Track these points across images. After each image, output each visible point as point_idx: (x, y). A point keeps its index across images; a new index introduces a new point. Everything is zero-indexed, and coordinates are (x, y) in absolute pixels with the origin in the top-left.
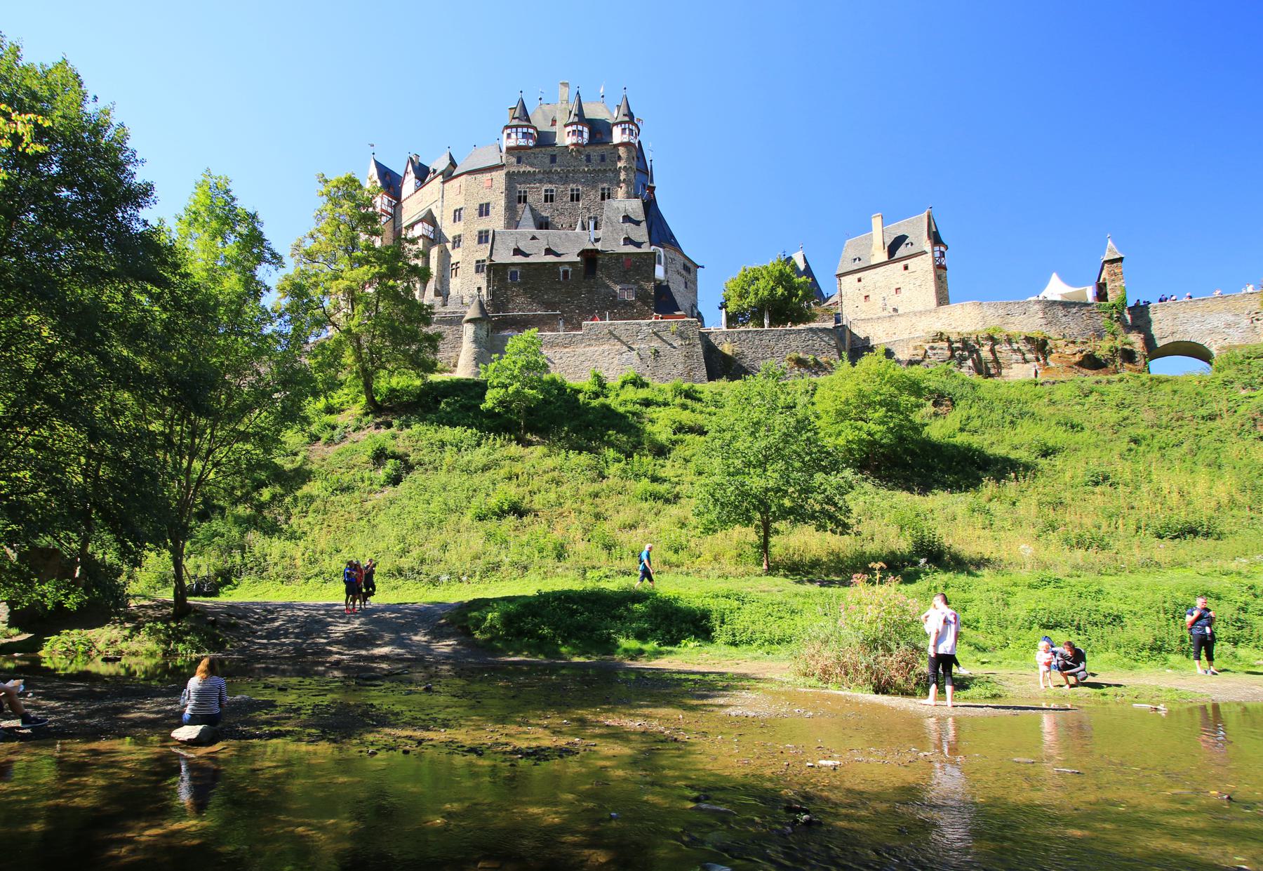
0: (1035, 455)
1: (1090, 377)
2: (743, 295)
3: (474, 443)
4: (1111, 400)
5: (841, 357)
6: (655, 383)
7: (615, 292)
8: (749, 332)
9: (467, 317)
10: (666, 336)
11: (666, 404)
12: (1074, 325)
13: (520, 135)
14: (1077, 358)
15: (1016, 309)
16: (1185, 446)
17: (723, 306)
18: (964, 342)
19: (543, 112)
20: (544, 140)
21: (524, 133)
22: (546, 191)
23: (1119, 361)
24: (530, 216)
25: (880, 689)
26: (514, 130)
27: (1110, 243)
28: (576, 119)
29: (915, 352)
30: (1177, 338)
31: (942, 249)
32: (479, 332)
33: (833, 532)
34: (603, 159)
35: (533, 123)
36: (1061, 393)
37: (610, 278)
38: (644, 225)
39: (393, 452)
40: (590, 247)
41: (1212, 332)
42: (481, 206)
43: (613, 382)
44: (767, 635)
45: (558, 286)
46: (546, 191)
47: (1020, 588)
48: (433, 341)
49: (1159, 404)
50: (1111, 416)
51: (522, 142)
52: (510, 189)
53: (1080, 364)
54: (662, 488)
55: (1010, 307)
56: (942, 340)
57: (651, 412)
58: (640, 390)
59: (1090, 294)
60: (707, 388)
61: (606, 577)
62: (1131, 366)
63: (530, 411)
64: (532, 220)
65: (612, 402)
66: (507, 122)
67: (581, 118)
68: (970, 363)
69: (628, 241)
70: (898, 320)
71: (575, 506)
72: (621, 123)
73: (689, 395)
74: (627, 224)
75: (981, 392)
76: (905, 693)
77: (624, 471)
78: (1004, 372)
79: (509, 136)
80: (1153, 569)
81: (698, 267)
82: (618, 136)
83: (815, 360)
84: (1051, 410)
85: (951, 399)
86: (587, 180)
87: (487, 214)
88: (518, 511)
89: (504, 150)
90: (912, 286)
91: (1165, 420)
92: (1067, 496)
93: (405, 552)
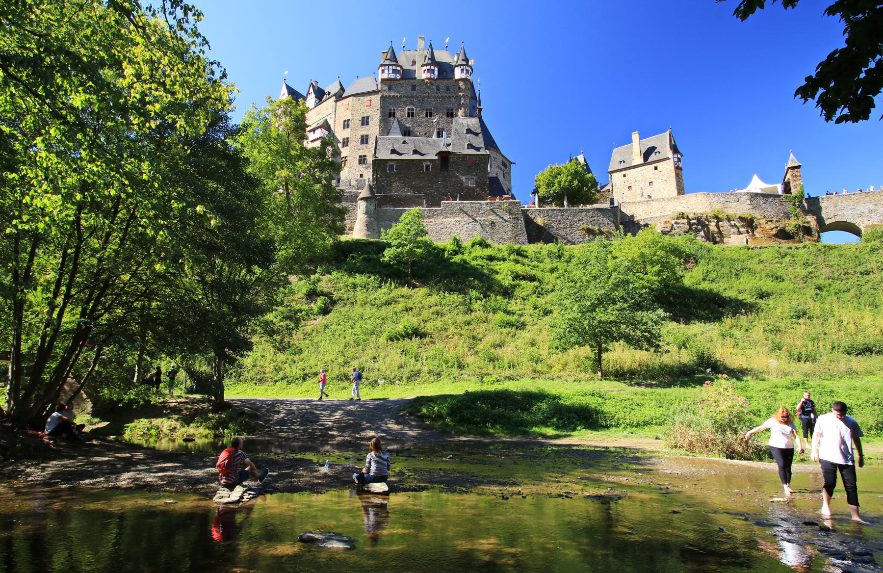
0: (755, 297)
1: (785, 245)
2: (550, 184)
3: (377, 285)
4: (800, 260)
6: (495, 245)
7: (462, 181)
8: (554, 210)
9: (361, 196)
10: (499, 212)
11: (504, 260)
12: (771, 210)
13: (391, 71)
14: (774, 232)
15: (732, 198)
16: (852, 292)
17: (536, 191)
19: (406, 56)
20: (408, 75)
21: (393, 70)
22: (409, 109)
23: (801, 234)
24: (398, 126)
26: (387, 67)
27: (791, 155)
28: (430, 62)
29: (665, 226)
30: (838, 219)
31: (679, 156)
32: (369, 206)
33: (647, 350)
34: (448, 89)
35: (400, 63)
36: (766, 255)
37: (458, 171)
38: (481, 135)
39: (322, 291)
40: (444, 149)
41: (860, 215)
42: (363, 118)
43: (466, 244)
45: (422, 176)
46: (409, 109)
47: (780, 389)
48: (342, 213)
49: (831, 264)
50: (801, 271)
51: (392, 76)
52: (383, 108)
53: (776, 236)
54: (513, 318)
55: (728, 196)
56: (683, 218)
57: (496, 265)
58: (485, 250)
59: (779, 189)
60: (531, 249)
61: (498, 381)
62: (809, 237)
63: (414, 263)
65: (466, 257)
66: (382, 63)
67: (433, 61)
68: (702, 233)
69: (470, 146)
71: (456, 331)
72: (460, 65)
73: (519, 253)
74: (469, 135)
75: (714, 254)
77: (484, 306)
78: (725, 240)
79: (383, 71)
80: (854, 376)
81: (512, 163)
82: (458, 74)
83: (599, 230)
84: (761, 266)
85: (695, 259)
86: (437, 103)
87: (367, 124)
88: (416, 333)
89: (379, 80)
90: (660, 181)
91: (836, 274)
92: (782, 325)
93: (346, 363)
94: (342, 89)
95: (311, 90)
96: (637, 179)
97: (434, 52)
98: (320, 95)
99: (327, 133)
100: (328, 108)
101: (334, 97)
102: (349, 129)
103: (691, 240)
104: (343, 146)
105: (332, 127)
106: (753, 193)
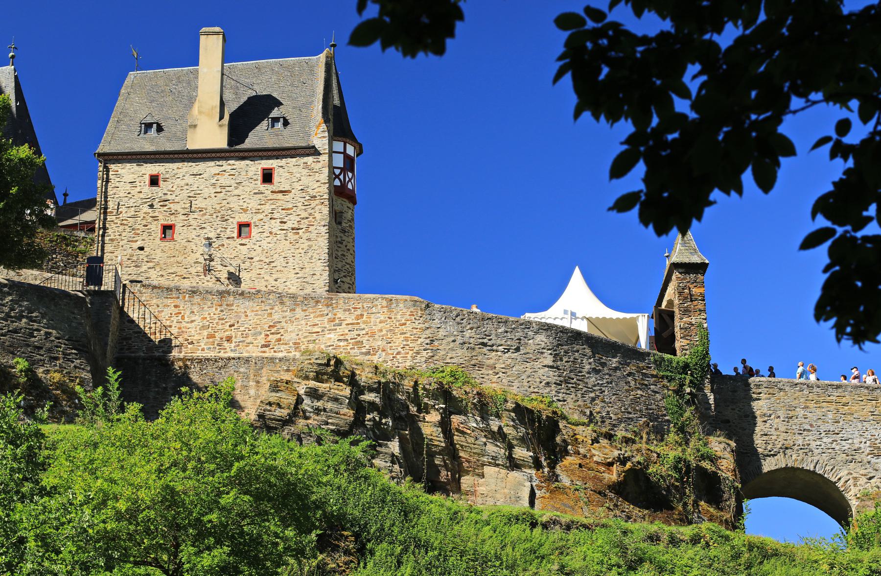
5: (99, 379)
14: (613, 475)
15: (497, 333)
18: (387, 390)
29: (273, 397)
31: (350, 150)
41: (852, 457)
55: (489, 327)
56: (339, 379)
68: (394, 446)
70: (241, 306)
75: (423, 529)
78: (466, 481)
90: (276, 225)
96: (199, 203)
103: (353, 467)
106: (563, 330)
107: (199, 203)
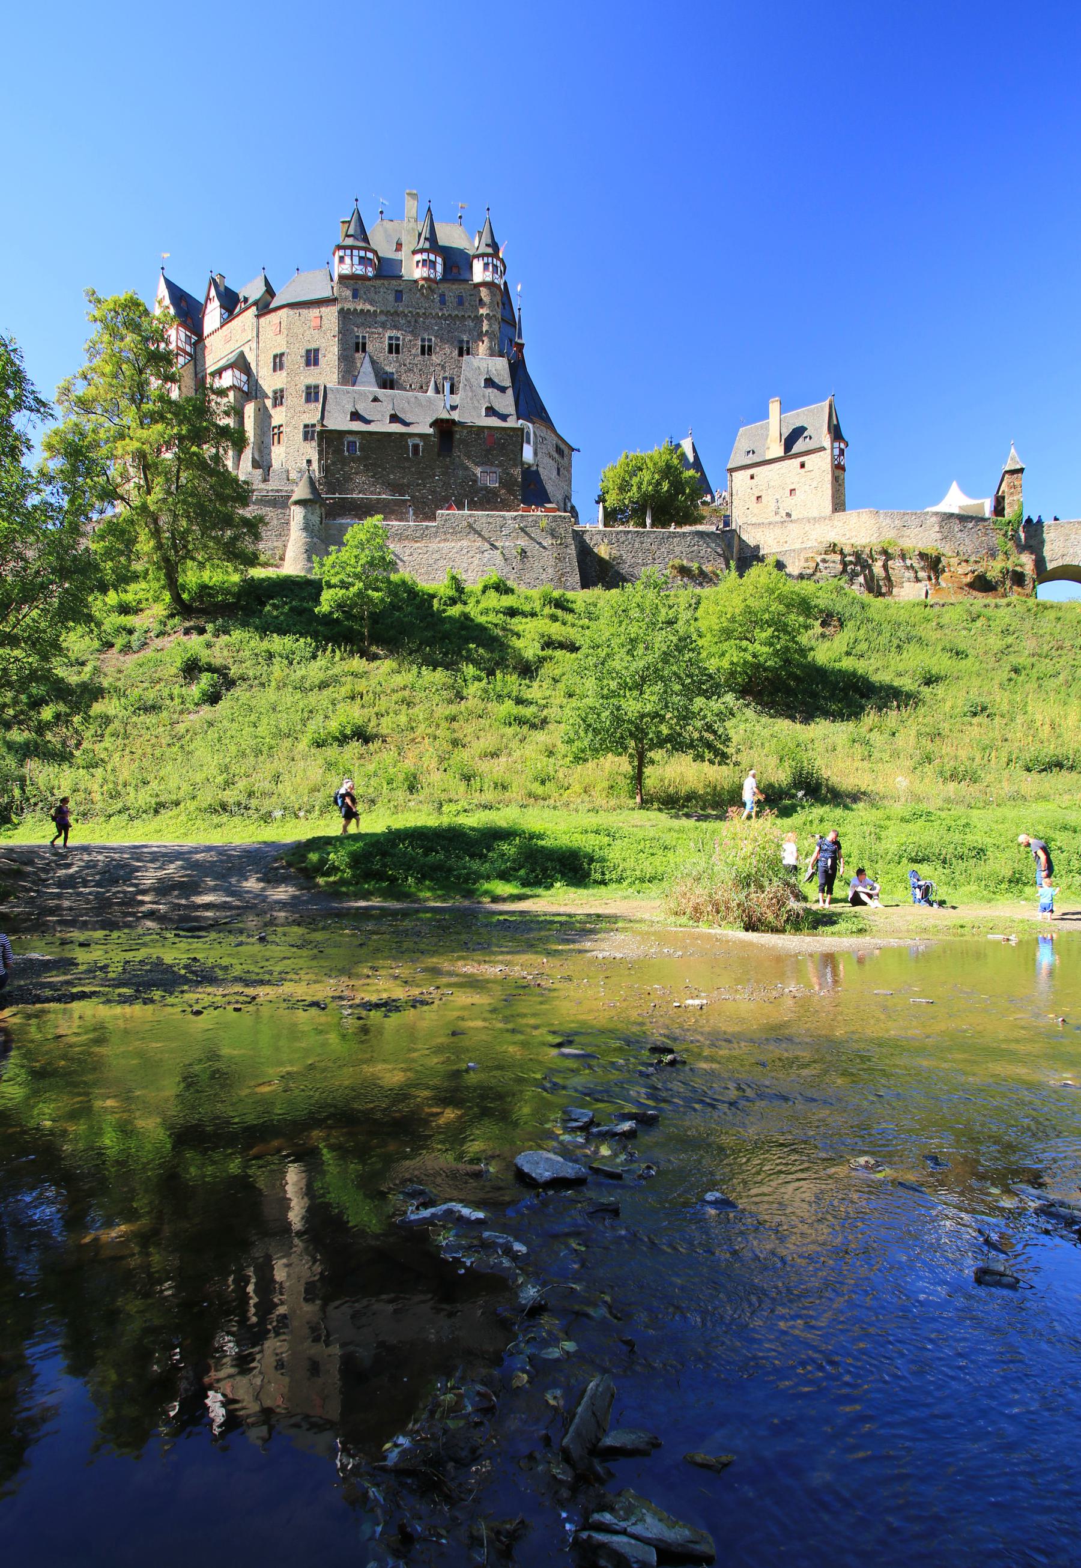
0: (919, 682)
1: (979, 600)
2: (624, 487)
3: (308, 655)
4: (997, 626)
5: (728, 567)
6: (522, 589)
7: (475, 475)
8: (629, 532)
9: (295, 497)
10: (534, 532)
11: (533, 614)
12: (968, 541)
13: (356, 260)
14: (969, 579)
15: (913, 522)
16: (1061, 677)
17: (601, 500)
18: (857, 555)
19: (386, 231)
20: (386, 270)
21: (361, 258)
22: (390, 338)
23: (1008, 583)
24: (370, 369)
25: (750, 927)
26: (348, 252)
28: (427, 245)
29: (806, 565)
30: (1067, 561)
31: (842, 446)
32: (310, 516)
34: (461, 301)
35: (373, 245)
36: (950, 616)
37: (469, 458)
38: (510, 392)
39: (209, 664)
40: (445, 415)
42: (308, 352)
43: (473, 584)
44: (638, 873)
45: (407, 464)
46: (390, 338)
48: (253, 527)
49: (1041, 632)
50: (995, 642)
51: (359, 270)
52: (344, 332)
53: (971, 585)
54: (528, 712)
55: (906, 517)
56: (835, 553)
57: (517, 624)
58: (504, 597)
59: (987, 507)
60: (580, 597)
61: (465, 811)
62: (1019, 590)
63: (375, 618)
64: (373, 375)
65: (472, 609)
66: (340, 240)
68: (861, 579)
69: (491, 411)
70: (791, 526)
71: (429, 731)
72: (483, 255)
73: (560, 604)
74: (490, 390)
75: (872, 613)
76: (775, 930)
77: (486, 691)
78: (895, 591)
79: (342, 259)
81: (573, 450)
82: (479, 273)
83: (700, 569)
84: (938, 634)
85: (839, 619)
86: (441, 328)
87: (316, 363)
88: (363, 735)
89: (336, 277)
90: (807, 487)
91: (1046, 648)
92: (945, 726)
93: (228, 784)
94: (270, 292)
95: (213, 293)
96: (772, 484)
97: (438, 227)
98: (230, 302)
99: (244, 378)
100: (244, 330)
101: (254, 308)
102: (284, 373)
103: (839, 590)
104: (275, 406)
105: (253, 366)
106: (945, 514)
107: (772, 484)
